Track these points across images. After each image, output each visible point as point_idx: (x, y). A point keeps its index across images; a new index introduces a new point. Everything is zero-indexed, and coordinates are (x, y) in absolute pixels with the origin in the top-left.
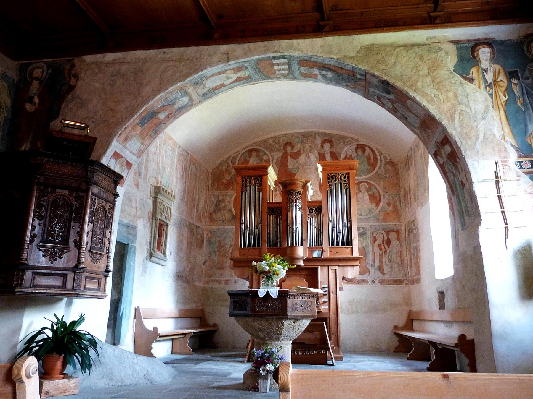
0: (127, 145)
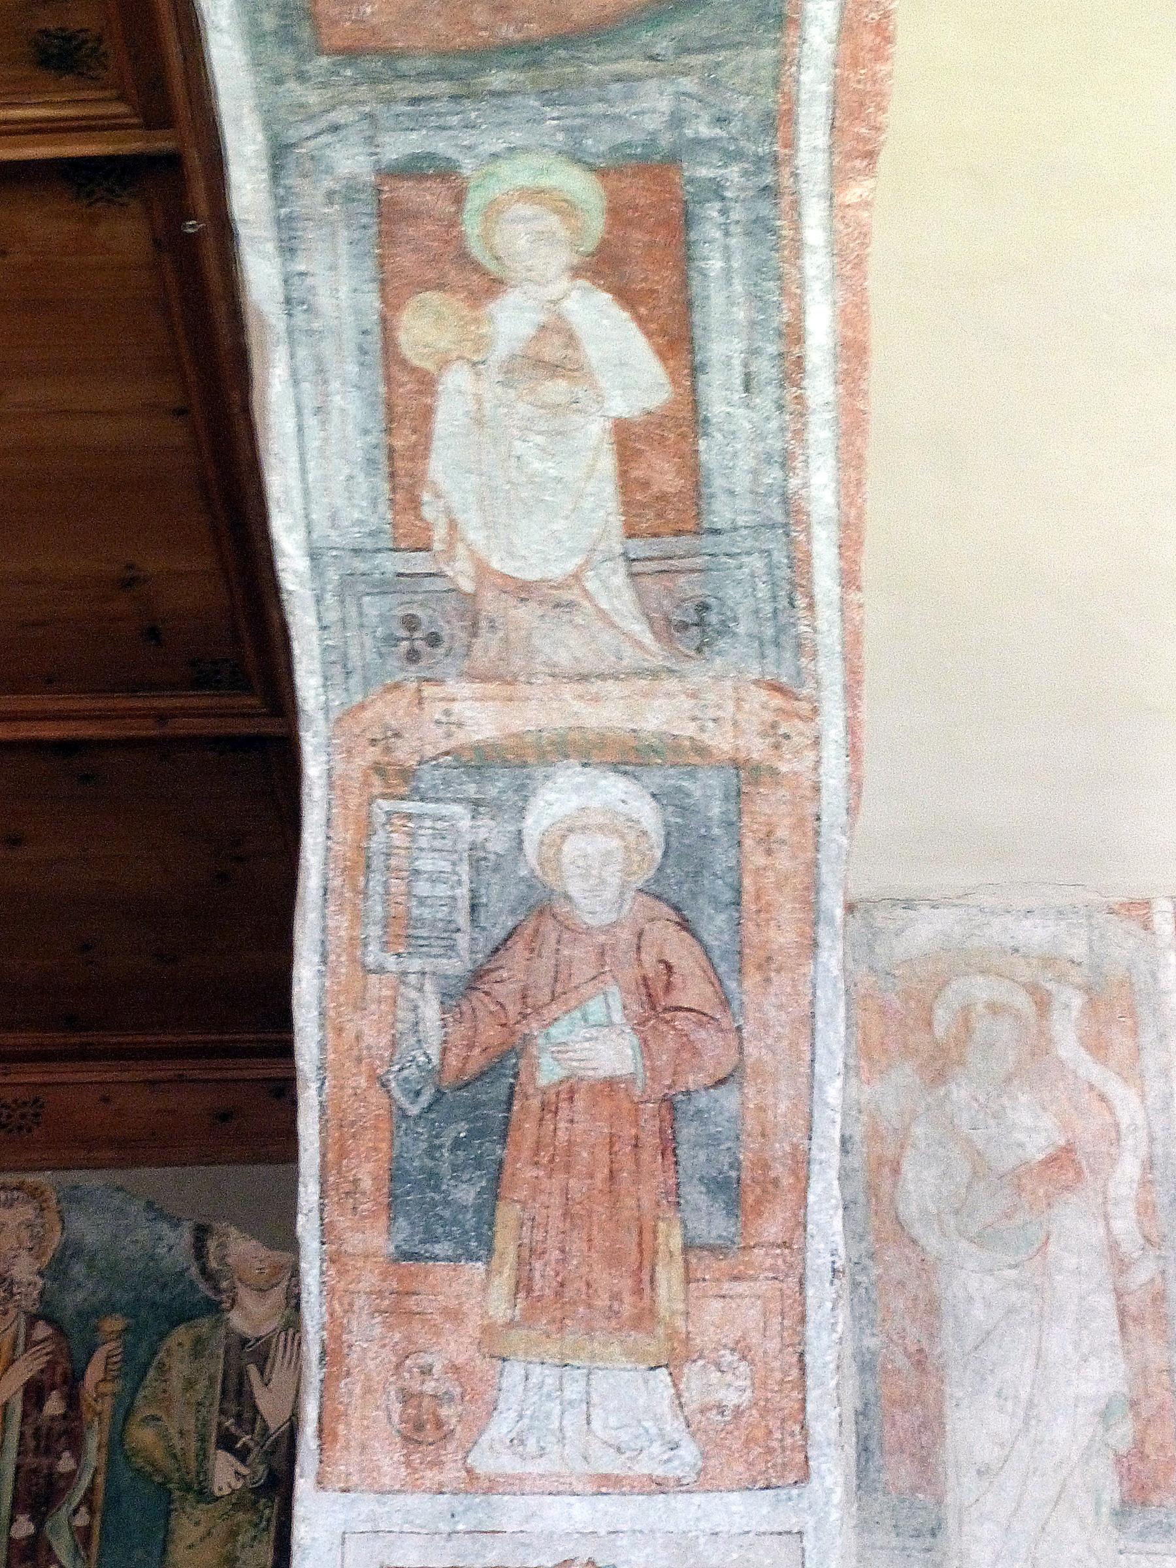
0: (484, 1461)
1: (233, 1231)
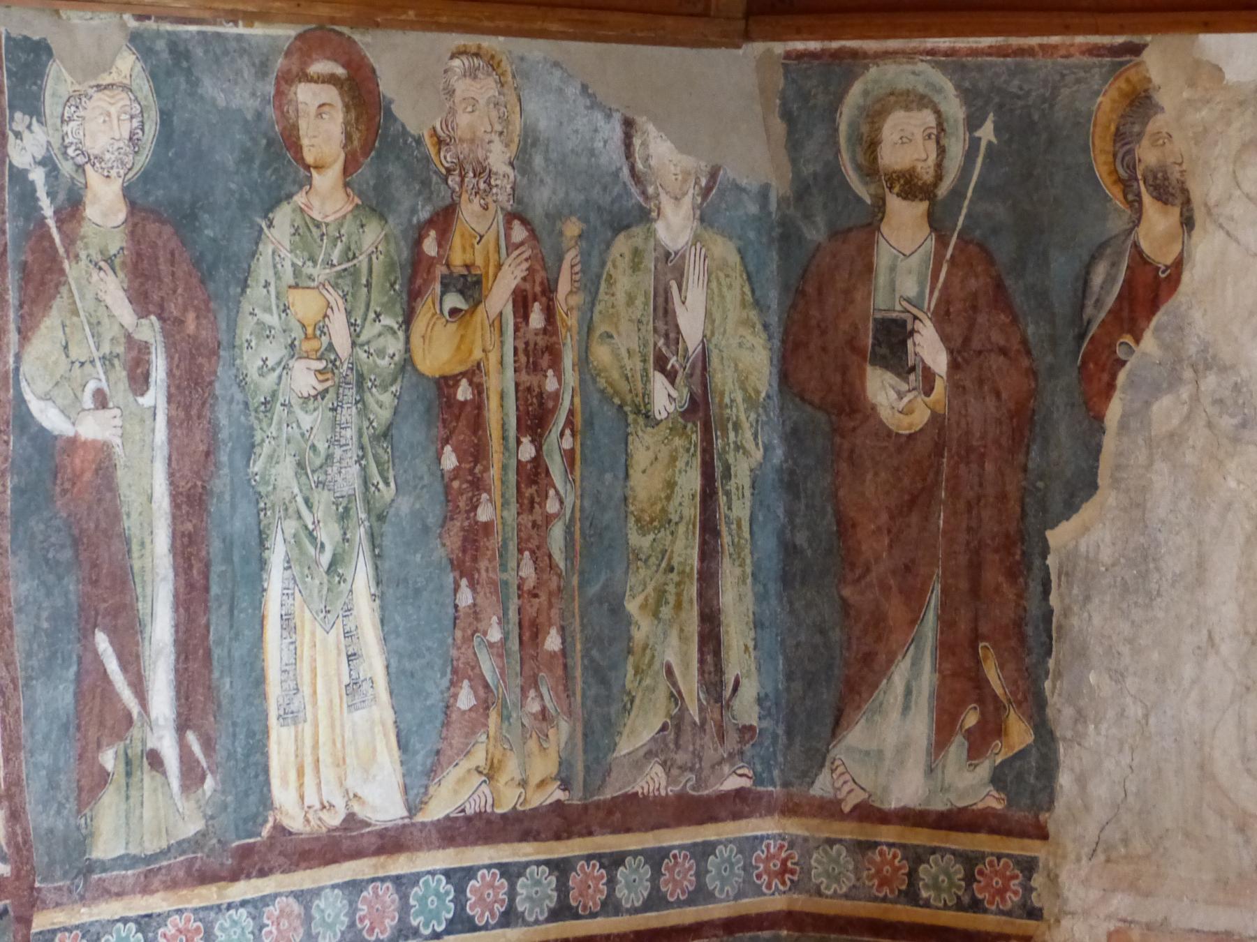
1: (651, 127)
